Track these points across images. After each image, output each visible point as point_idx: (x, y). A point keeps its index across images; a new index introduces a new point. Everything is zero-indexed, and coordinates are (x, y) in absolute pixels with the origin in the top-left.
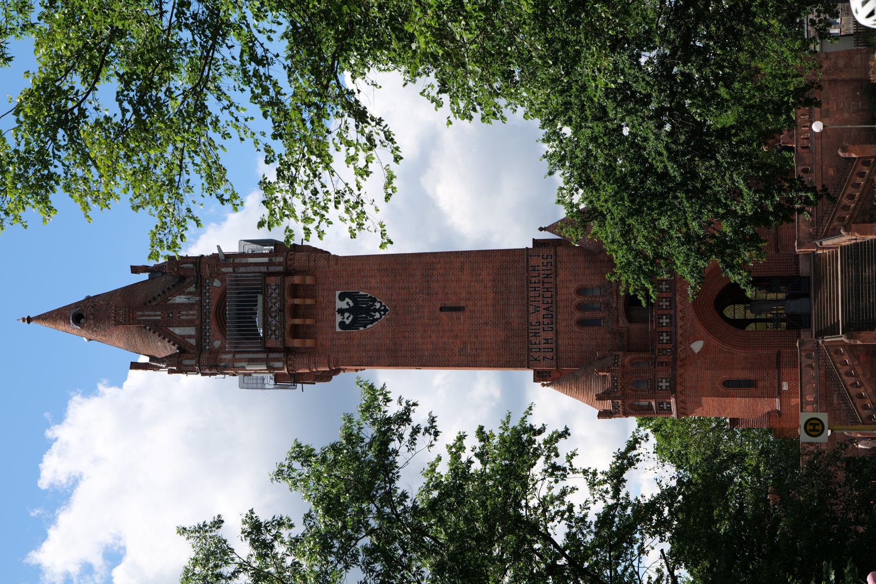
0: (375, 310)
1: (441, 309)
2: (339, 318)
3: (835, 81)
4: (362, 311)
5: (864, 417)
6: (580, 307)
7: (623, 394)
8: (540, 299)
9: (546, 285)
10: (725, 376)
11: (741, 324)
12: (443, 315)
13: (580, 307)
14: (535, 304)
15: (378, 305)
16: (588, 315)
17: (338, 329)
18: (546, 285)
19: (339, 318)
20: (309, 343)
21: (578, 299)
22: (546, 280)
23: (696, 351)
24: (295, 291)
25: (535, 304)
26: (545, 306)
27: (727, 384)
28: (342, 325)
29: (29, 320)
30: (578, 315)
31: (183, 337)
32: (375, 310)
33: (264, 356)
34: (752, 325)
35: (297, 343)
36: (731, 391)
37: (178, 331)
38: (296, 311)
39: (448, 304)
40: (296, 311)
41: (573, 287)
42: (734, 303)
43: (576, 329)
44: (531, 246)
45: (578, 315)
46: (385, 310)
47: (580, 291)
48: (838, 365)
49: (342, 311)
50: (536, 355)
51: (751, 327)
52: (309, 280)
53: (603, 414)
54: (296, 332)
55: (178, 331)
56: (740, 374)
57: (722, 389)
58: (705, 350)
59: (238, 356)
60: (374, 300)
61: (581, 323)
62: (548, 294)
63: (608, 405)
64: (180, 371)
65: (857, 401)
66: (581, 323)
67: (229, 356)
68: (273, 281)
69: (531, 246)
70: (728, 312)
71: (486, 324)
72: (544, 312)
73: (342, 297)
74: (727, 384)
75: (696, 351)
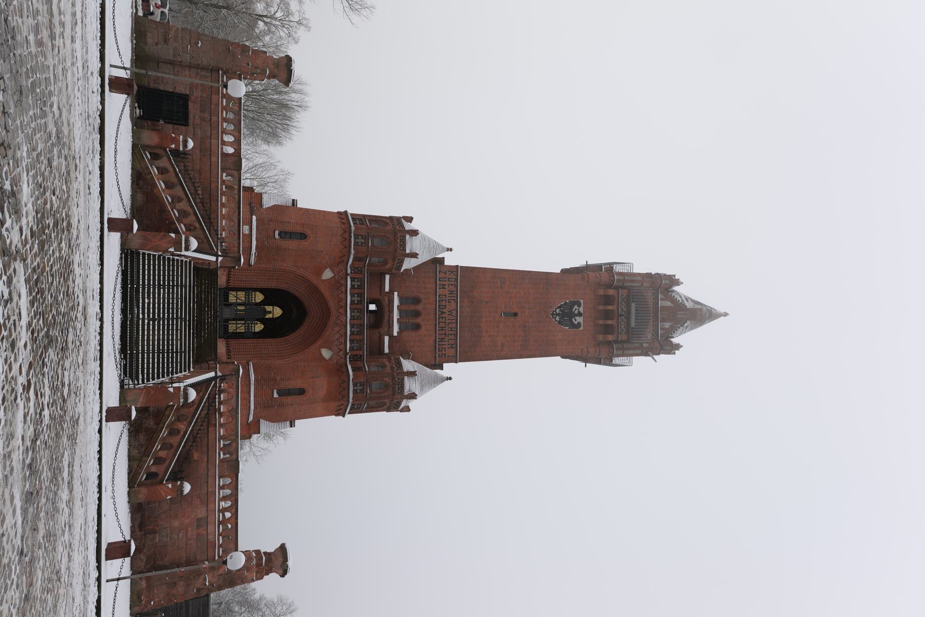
0: (559, 315)
1: (515, 314)
2: (581, 309)
3: (188, 563)
4: (567, 314)
5: (165, 159)
6: (417, 314)
7: (395, 234)
8: (448, 321)
9: (443, 332)
10: (304, 243)
11: (273, 296)
12: (516, 311)
13: (417, 314)
14: (451, 317)
15: (557, 319)
16: (412, 307)
17: (582, 301)
18: (443, 332)
19: (581, 309)
20: (601, 292)
21: (419, 320)
22: (443, 336)
23: (328, 270)
24: (608, 330)
25: (451, 317)
26: (444, 315)
27: (303, 236)
28: (579, 306)
29: (726, 314)
30: (419, 307)
31: (667, 300)
32: (559, 315)
33: (627, 284)
34: (258, 301)
35: (611, 292)
36: (299, 229)
37: (669, 304)
38: (608, 315)
39: (512, 319)
40: (608, 315)
41: (422, 331)
42: (273, 318)
43: (422, 296)
44: (445, 365)
45: (419, 307)
46: (553, 315)
47: (417, 327)
48: (197, 225)
49: (580, 314)
50: (452, 276)
51: (259, 297)
52: (601, 338)
53: (410, 219)
54: (608, 300)
55: (669, 304)
56: (292, 244)
57: (308, 232)
58: (319, 272)
59: (639, 284)
60: (559, 322)
61: (417, 301)
62: (442, 325)
63: (408, 226)
64: (670, 276)
65: (174, 180)
66: (417, 301)
67: (645, 285)
68: (623, 337)
69: (445, 365)
70: (277, 312)
71: (487, 302)
72: (445, 310)
73: (579, 323)
74: (303, 236)
75: (328, 270)
